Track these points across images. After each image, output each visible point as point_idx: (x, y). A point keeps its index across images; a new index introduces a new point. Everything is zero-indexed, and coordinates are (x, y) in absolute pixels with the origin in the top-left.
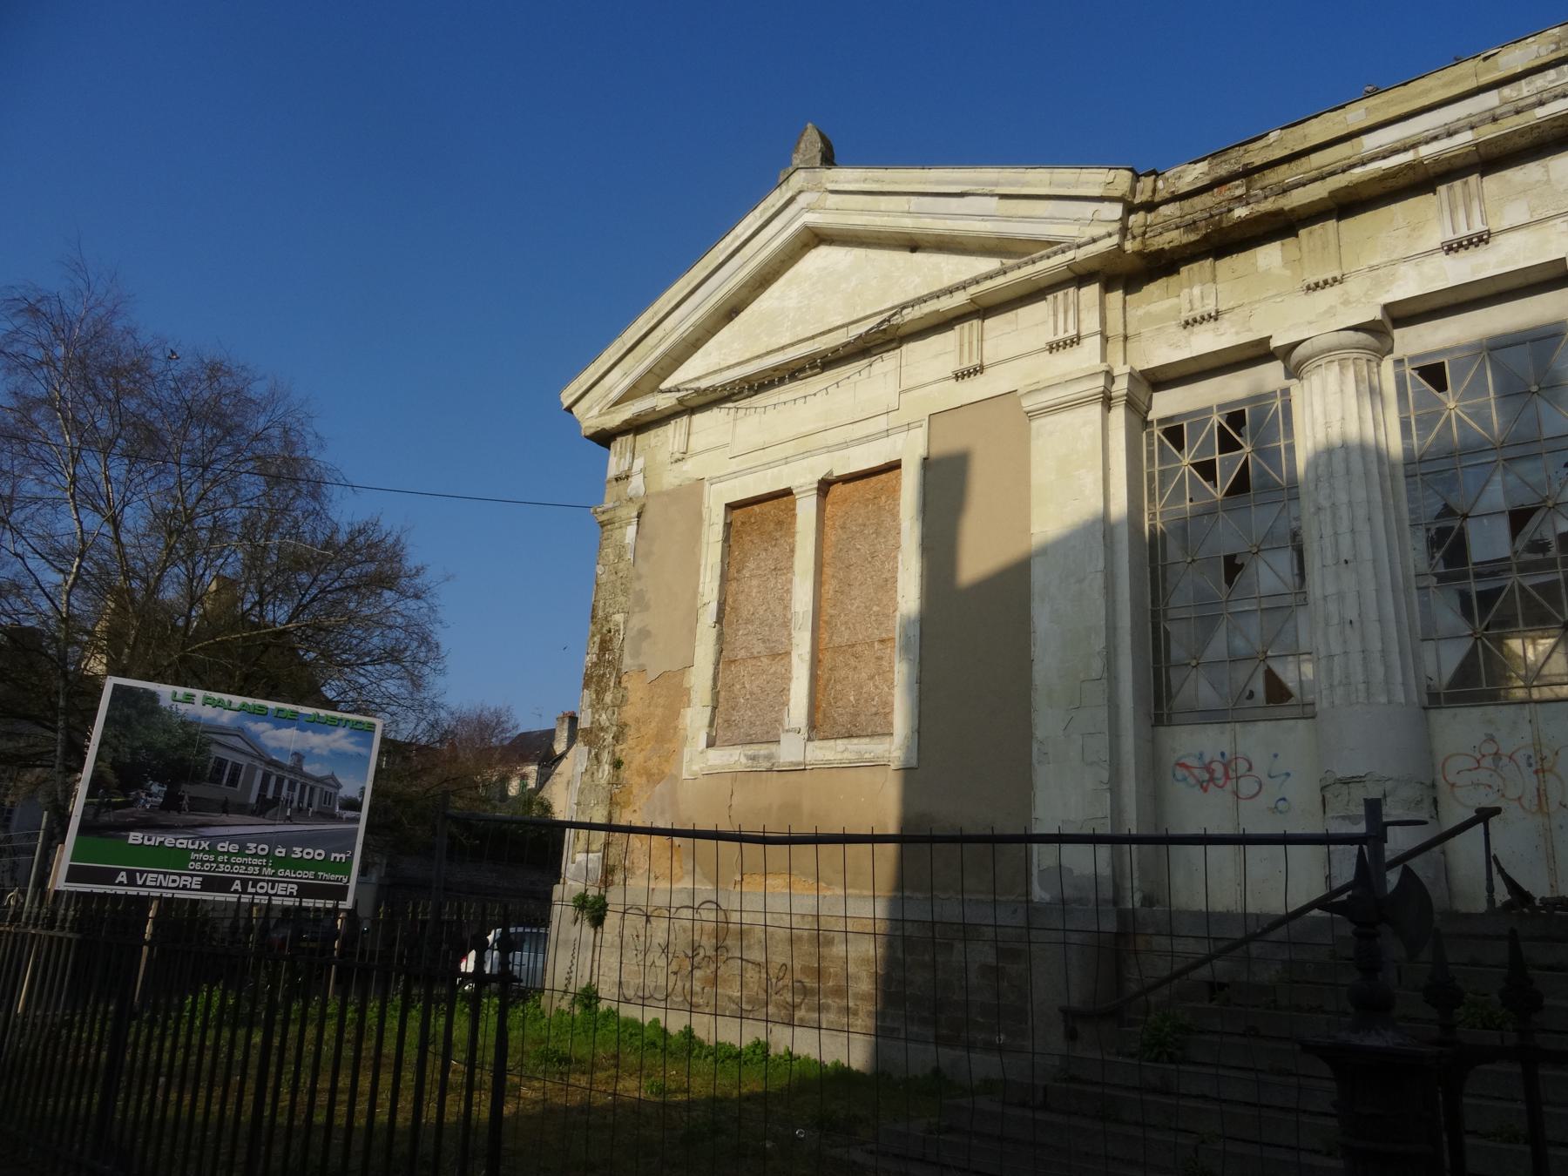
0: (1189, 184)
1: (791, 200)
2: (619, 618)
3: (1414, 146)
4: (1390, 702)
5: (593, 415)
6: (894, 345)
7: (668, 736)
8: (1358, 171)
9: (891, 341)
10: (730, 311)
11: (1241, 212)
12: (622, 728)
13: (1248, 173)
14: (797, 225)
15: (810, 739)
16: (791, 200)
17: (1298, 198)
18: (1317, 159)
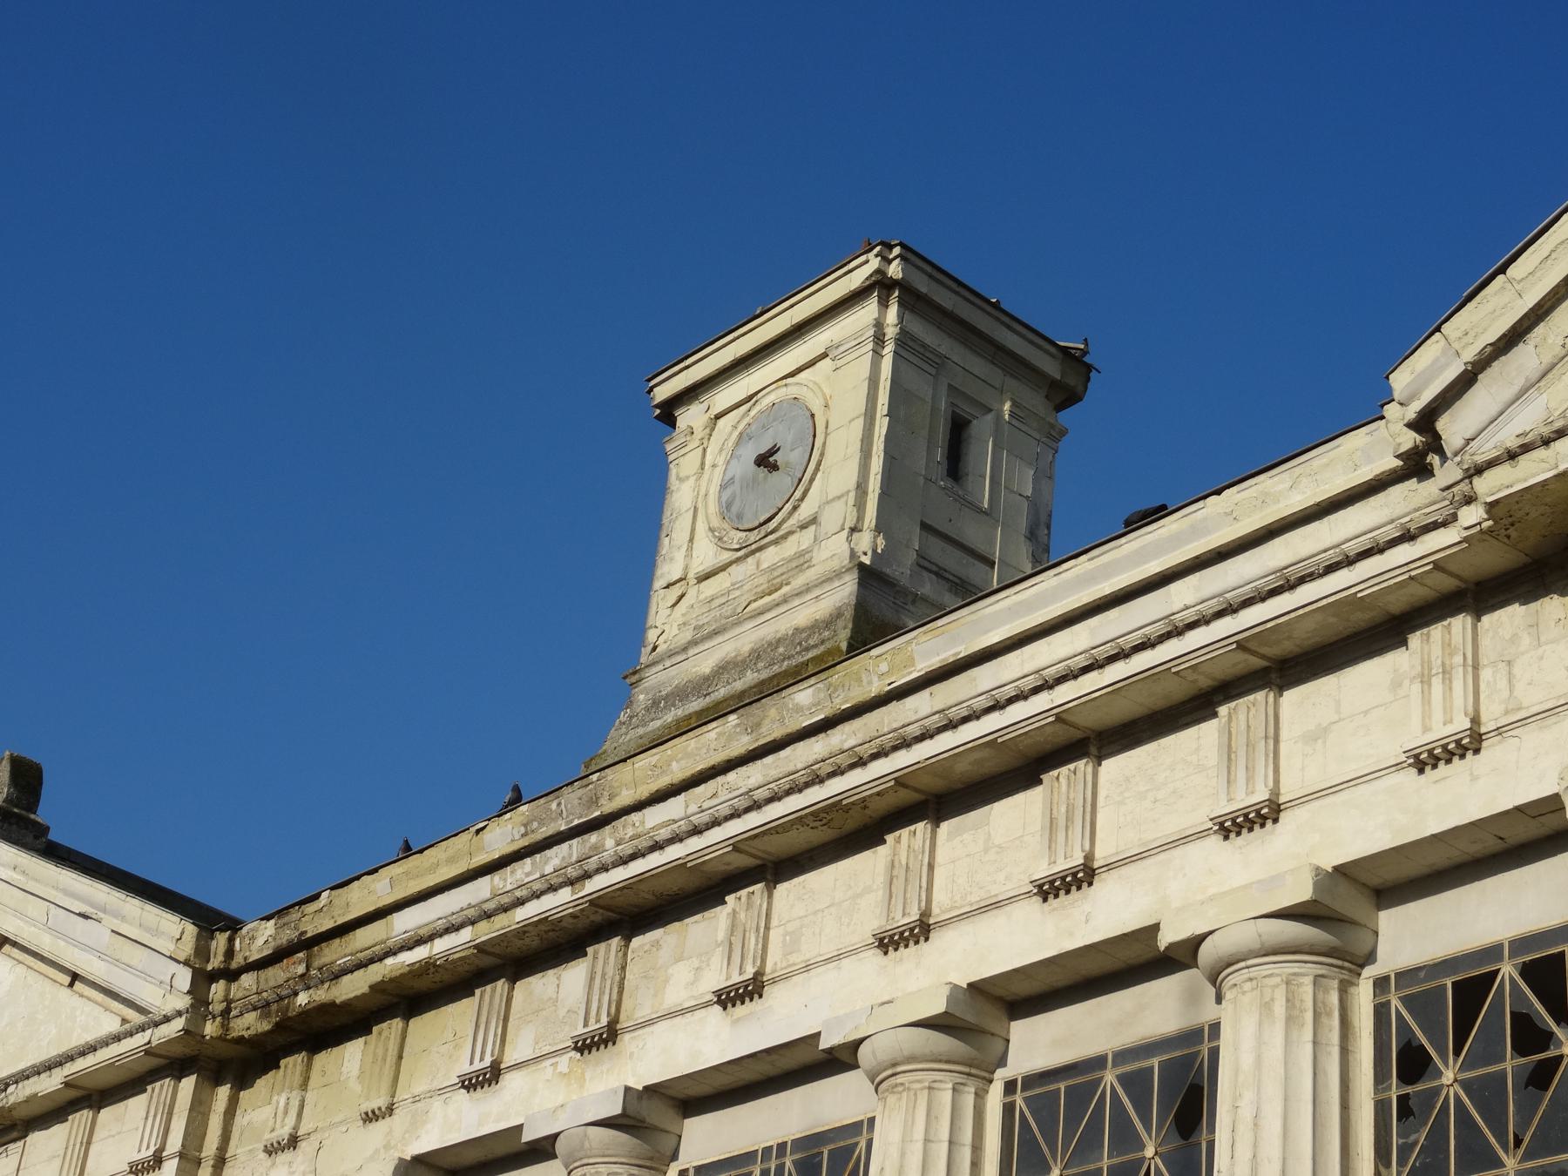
0: (261, 950)
3: (431, 938)
6: (15, 1134)
8: (390, 961)
9: (13, 1127)
11: (302, 999)
13: (309, 944)
17: (353, 987)
18: (364, 938)
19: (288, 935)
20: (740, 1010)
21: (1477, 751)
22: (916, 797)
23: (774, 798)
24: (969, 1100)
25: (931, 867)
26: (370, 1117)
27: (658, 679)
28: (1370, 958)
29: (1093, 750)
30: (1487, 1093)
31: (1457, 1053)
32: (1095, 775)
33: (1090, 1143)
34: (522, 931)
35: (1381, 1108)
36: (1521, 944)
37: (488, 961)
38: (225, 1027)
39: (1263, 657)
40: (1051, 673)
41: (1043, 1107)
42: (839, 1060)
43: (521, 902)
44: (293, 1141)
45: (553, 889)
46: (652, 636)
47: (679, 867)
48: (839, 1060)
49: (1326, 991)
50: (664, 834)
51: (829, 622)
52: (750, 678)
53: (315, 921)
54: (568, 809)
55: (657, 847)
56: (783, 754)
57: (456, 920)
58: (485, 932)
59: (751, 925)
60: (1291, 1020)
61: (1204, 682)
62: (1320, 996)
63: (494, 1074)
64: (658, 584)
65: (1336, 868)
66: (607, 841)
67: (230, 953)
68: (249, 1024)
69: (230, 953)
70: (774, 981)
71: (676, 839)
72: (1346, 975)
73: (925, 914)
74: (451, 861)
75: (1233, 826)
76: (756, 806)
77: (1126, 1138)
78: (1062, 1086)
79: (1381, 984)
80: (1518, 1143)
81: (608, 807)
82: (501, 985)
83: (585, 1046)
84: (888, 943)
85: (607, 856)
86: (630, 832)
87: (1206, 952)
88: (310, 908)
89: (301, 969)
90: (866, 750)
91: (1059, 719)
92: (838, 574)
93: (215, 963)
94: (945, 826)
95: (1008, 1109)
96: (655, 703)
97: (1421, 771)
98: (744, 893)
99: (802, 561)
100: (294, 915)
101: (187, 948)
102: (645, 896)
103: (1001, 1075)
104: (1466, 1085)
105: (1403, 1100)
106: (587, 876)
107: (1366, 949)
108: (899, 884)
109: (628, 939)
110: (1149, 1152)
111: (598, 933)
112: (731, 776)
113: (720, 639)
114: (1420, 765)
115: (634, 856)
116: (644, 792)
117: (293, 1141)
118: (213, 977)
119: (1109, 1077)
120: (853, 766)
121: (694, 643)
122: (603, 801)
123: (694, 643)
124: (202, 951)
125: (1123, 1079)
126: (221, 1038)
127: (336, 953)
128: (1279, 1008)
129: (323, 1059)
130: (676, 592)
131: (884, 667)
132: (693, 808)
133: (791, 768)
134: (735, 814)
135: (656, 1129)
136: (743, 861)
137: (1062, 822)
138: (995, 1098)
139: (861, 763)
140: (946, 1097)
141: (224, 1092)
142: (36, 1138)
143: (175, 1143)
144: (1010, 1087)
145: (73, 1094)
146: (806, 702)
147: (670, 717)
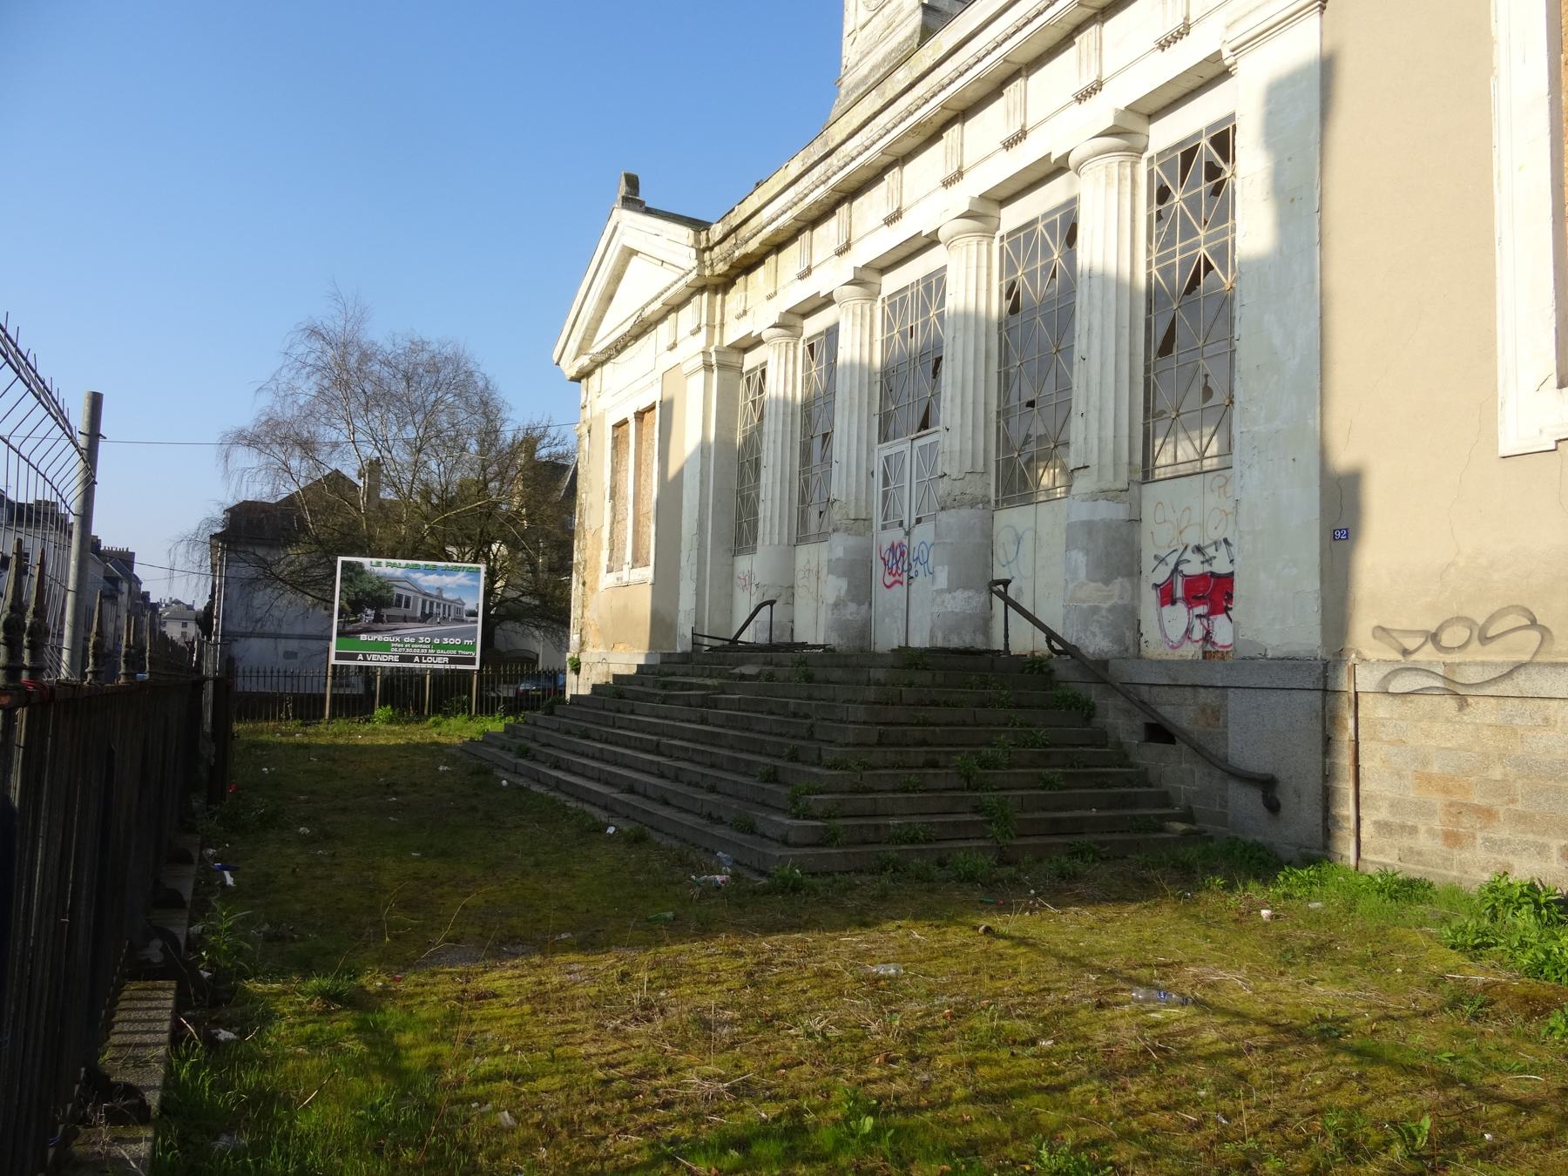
1: (615, 228)
2: (584, 496)
4: (770, 544)
5: (570, 368)
7: (596, 569)
8: (764, 231)
10: (608, 298)
12: (585, 561)
14: (620, 245)
15: (633, 567)
16: (615, 228)
17: (753, 245)
18: (754, 223)
19: (727, 228)
20: (894, 225)
21: (1188, 34)
22: (953, 113)
23: (895, 126)
24: (984, 247)
25: (962, 145)
26: (769, 297)
27: (849, 81)
28: (1146, 148)
29: (1024, 73)
30: (1193, 203)
31: (1181, 186)
32: (1026, 85)
33: (1033, 257)
34: (809, 208)
35: (1149, 217)
36: (1210, 128)
37: (800, 224)
38: (713, 271)
39: (1093, 8)
40: (1000, 39)
41: (1015, 245)
42: (932, 241)
43: (806, 195)
44: (745, 312)
45: (817, 187)
46: (844, 61)
47: (863, 167)
48: (932, 241)
49: (1125, 168)
50: (855, 153)
51: (910, 37)
52: (882, 71)
53: (735, 220)
54: (818, 149)
55: (853, 159)
56: (896, 104)
57: (784, 208)
58: (795, 211)
59: (895, 188)
60: (1107, 184)
61: (1068, 28)
62: (1122, 171)
63: (809, 271)
64: (845, 35)
65: (1127, 108)
66: (834, 161)
67: (708, 240)
68: (721, 268)
69: (708, 240)
70: (905, 210)
71: (860, 154)
72: (1134, 159)
73: (960, 167)
74: (778, 183)
75: (1082, 97)
76: (888, 131)
77: (1047, 251)
78: (1022, 234)
79: (1151, 160)
80: (1206, 222)
81: (832, 145)
82: (807, 233)
83: (839, 253)
84: (947, 183)
85: (835, 169)
86: (842, 155)
87: (1072, 161)
88: (732, 215)
89: (734, 241)
90: (928, 96)
91: (1005, 61)
92: (914, 11)
93: (703, 245)
94: (968, 124)
95: (1001, 248)
96: (848, 93)
97: (1163, 50)
98: (891, 173)
99: (899, 9)
100: (727, 218)
101: (691, 241)
102: (854, 184)
103: (998, 234)
104: (1185, 200)
105: (1159, 212)
106: (829, 178)
107: (1141, 145)
108: (949, 156)
109: (851, 203)
110: (1056, 256)
111: (839, 203)
112: (877, 119)
113: (870, 55)
114: (1162, 47)
115: (845, 166)
116: (844, 136)
117: (745, 312)
118: (704, 251)
119: (1040, 227)
120: (924, 104)
121: (860, 60)
122: (830, 143)
123: (860, 60)
124: (697, 241)
125: (1046, 226)
126: (712, 275)
127: (745, 232)
128: (1103, 178)
129: (752, 276)
130: (852, 37)
131: (930, 52)
132: (864, 139)
133: (899, 111)
134: (881, 137)
135: (870, 283)
136: (888, 159)
137: (1012, 110)
138: (996, 243)
139: (927, 101)
140: (974, 248)
141: (719, 297)
142: (660, 327)
143: (704, 321)
144: (1002, 238)
145: (667, 308)
146: (902, 77)
147: (855, 95)
